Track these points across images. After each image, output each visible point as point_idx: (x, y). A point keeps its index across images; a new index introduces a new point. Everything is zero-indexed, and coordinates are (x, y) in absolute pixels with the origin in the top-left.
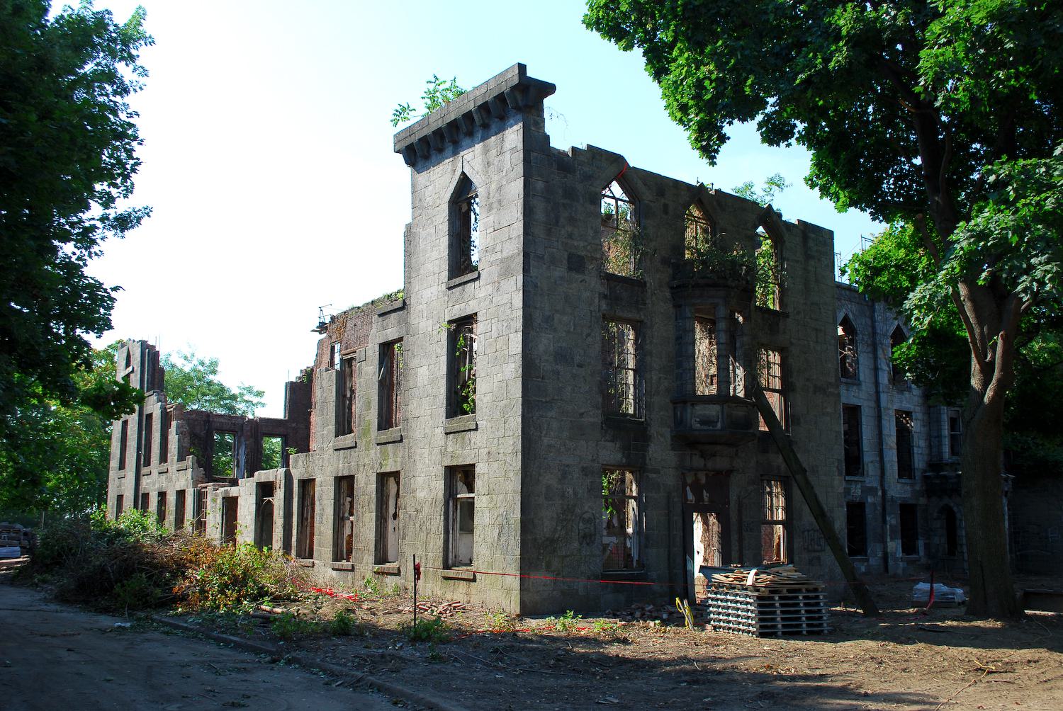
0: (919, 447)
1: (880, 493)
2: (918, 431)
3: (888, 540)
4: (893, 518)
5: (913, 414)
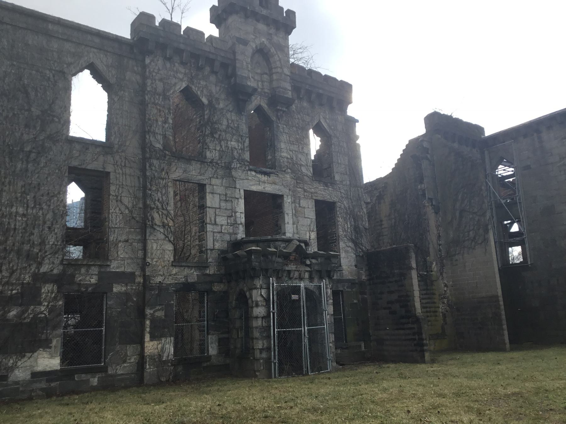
0: (215, 224)
1: (140, 280)
2: (217, 206)
3: (147, 337)
4: (159, 310)
5: (207, 186)
